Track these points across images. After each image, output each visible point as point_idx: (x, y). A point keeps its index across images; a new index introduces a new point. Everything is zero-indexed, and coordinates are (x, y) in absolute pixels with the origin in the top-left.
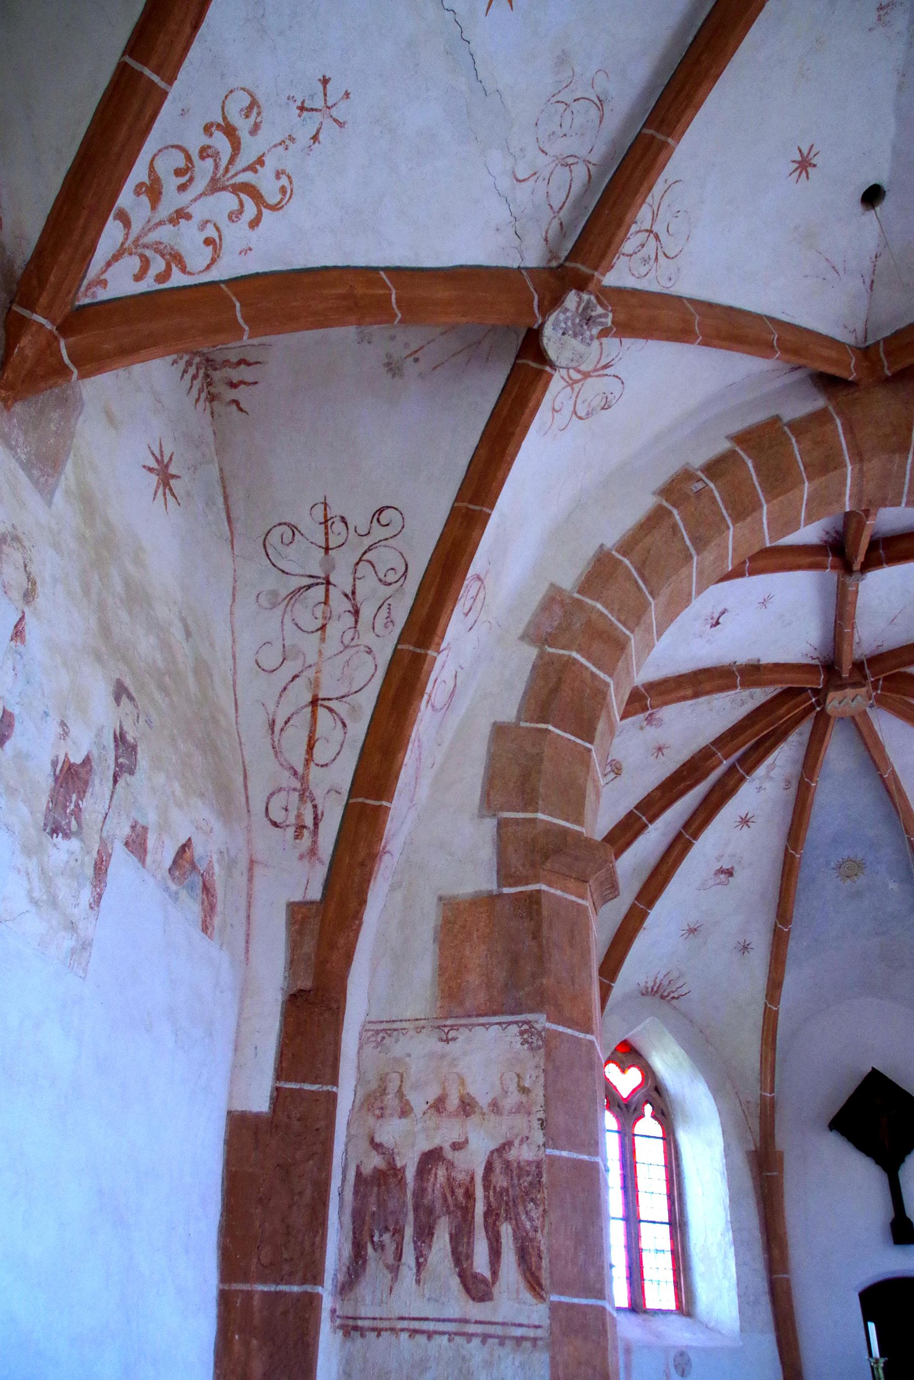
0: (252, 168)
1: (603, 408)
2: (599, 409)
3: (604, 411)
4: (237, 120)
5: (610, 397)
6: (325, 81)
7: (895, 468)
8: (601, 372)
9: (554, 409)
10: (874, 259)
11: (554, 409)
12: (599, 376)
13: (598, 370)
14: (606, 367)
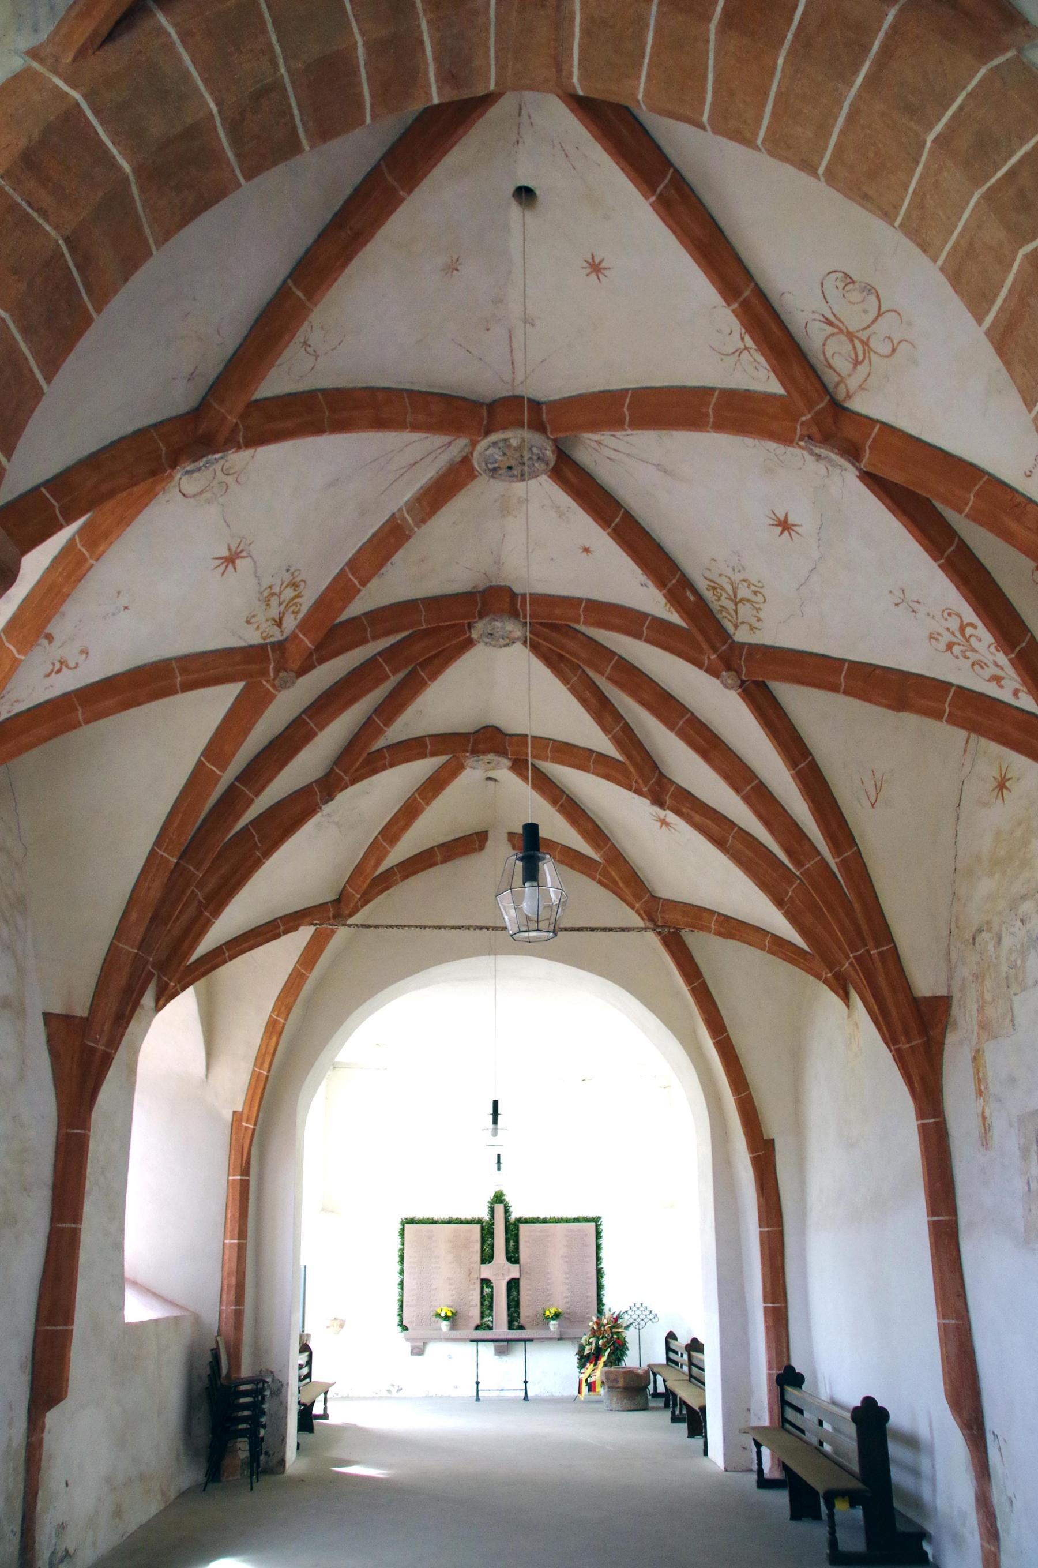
0: (953, 633)
1: (853, 282)
2: (857, 285)
3: (855, 279)
4: (942, 646)
5: (841, 285)
6: (897, 605)
7: (510, 64)
8: (837, 322)
9: (894, 351)
10: (521, 141)
11: (894, 351)
12: (841, 322)
13: (838, 327)
14: (830, 323)
